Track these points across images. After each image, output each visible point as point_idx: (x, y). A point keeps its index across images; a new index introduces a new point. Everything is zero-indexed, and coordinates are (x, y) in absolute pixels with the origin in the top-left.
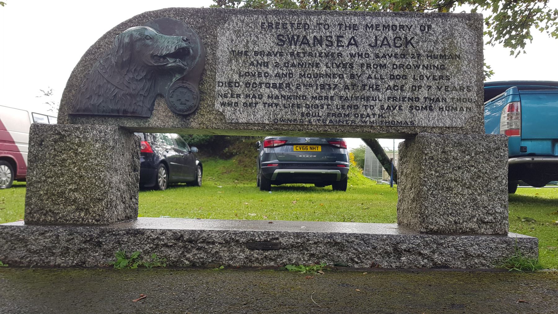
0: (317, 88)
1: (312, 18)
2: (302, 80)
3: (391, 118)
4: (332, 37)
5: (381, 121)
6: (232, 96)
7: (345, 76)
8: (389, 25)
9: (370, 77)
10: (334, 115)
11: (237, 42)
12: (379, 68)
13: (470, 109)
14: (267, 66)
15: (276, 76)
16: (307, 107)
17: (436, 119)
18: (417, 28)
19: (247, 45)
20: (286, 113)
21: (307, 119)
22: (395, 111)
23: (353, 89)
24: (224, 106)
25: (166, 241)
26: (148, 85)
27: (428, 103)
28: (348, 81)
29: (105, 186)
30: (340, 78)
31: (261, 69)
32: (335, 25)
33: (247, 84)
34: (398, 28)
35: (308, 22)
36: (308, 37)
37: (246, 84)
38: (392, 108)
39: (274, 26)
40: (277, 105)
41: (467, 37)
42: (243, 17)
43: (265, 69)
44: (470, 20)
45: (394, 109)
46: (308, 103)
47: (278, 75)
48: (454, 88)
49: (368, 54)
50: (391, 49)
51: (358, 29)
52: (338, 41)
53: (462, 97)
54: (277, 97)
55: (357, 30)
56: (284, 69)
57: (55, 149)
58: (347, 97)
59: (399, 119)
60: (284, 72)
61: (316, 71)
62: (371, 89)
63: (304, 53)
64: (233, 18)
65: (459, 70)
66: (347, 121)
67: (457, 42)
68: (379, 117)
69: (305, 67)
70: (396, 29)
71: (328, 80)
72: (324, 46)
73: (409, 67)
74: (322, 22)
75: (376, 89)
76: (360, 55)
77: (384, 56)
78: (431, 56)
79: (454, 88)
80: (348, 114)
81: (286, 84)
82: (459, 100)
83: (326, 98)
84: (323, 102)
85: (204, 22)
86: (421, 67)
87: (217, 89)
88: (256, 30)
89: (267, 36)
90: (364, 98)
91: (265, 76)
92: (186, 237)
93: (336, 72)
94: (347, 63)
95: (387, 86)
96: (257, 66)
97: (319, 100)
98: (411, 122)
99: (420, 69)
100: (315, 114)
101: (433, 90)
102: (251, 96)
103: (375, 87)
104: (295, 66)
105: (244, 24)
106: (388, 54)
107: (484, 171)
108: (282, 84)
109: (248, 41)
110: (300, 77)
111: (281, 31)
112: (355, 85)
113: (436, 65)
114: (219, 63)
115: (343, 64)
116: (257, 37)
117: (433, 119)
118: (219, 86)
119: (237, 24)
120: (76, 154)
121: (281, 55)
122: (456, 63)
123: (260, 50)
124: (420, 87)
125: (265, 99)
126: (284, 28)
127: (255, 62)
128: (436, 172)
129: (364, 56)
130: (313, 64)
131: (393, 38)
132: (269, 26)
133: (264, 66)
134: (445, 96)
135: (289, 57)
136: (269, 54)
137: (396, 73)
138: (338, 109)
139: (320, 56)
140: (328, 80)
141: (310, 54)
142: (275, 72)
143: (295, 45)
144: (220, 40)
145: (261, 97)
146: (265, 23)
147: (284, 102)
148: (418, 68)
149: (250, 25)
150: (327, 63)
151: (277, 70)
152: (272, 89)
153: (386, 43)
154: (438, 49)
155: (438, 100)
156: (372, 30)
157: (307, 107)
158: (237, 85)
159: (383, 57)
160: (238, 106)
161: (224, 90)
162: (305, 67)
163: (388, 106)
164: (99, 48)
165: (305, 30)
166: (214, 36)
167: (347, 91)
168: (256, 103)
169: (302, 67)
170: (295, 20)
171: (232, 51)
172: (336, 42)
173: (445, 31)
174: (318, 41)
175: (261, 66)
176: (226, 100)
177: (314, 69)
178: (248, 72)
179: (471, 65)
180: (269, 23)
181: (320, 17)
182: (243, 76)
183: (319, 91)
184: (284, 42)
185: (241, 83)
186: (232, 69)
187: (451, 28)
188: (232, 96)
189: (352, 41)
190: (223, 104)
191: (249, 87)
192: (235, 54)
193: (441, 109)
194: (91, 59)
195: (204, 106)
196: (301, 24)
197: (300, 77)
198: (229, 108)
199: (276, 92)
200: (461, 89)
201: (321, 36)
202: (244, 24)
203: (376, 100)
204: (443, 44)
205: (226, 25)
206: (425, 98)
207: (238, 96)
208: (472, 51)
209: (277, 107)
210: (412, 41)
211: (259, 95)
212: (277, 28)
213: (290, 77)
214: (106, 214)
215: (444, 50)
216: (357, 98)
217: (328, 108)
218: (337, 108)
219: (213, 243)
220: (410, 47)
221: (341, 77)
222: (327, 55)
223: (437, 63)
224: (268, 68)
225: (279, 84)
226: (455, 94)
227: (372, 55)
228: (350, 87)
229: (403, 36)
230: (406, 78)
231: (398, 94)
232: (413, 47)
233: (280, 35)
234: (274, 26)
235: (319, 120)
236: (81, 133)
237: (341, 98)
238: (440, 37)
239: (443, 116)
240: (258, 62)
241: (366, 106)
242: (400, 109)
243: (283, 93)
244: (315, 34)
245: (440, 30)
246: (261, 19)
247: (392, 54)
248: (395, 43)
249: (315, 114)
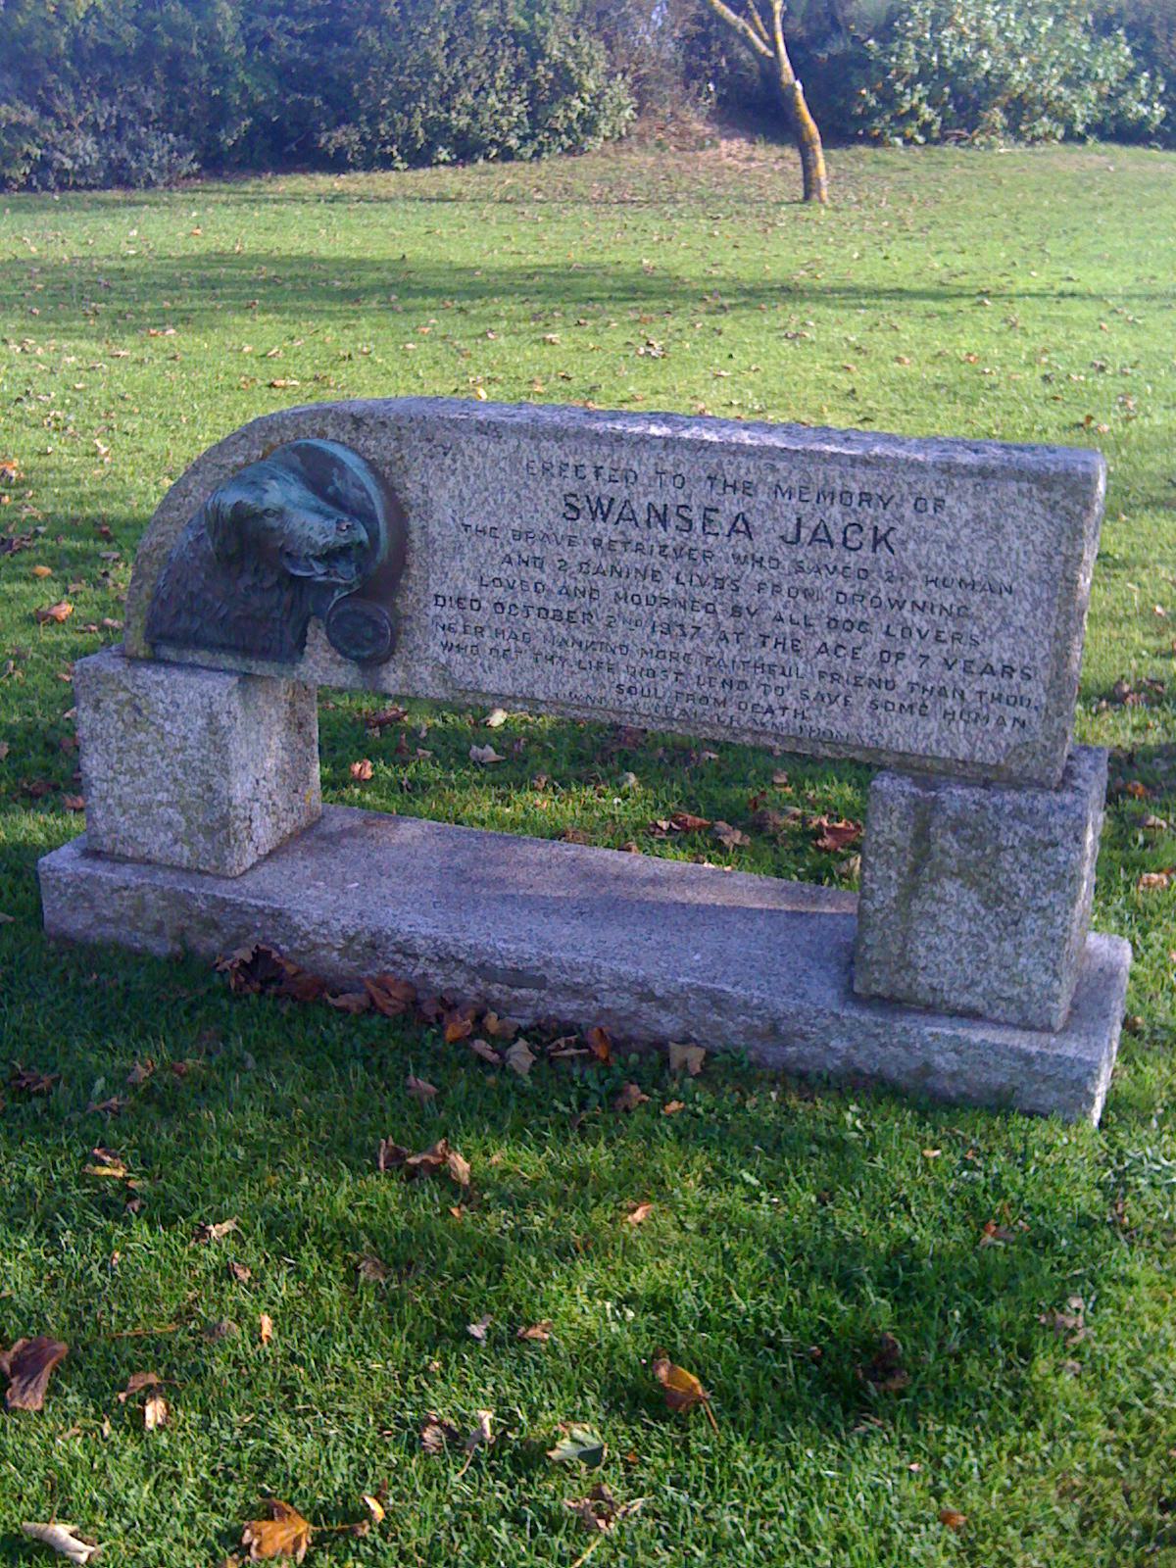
7: (719, 608)
10: (691, 697)
13: (1023, 724)
17: (934, 737)
20: (584, 681)
22: (834, 706)
26: (287, 598)
27: (916, 697)
28: (728, 624)
35: (635, 468)
41: (1037, 537)
48: (989, 670)
50: (834, 554)
53: (1006, 692)
56: (580, 576)
59: (842, 728)
63: (626, 543)
65: (1006, 624)
72: (671, 530)
74: (668, 467)
79: (989, 670)
80: (724, 702)
83: (674, 656)
84: (666, 664)
86: (908, 606)
91: (536, 590)
95: (818, 644)
99: (906, 612)
101: (934, 667)
103: (789, 643)
107: (1014, 890)
111: (571, 484)
117: (927, 736)
119: (472, 459)
123: (525, 528)
124: (900, 656)
127: (514, 556)
131: (841, 525)
132: (545, 470)
134: (961, 685)
137: (842, 614)
141: (639, 548)
142: (560, 584)
147: (580, 656)
153: (822, 535)
155: (942, 692)
167: (723, 644)
170: (601, 454)
179: (1039, 613)
183: (657, 637)
185: (484, 604)
189: (740, 523)
190: (447, 647)
199: (561, 630)
205: (448, 461)
206: (912, 686)
208: (1046, 576)
210: (890, 538)
219: (416, 957)
226: (988, 683)
227: (786, 564)
231: (845, 665)
234: (555, 471)
243: (579, 636)
244: (651, 498)
245: (966, 513)
248: (845, 540)
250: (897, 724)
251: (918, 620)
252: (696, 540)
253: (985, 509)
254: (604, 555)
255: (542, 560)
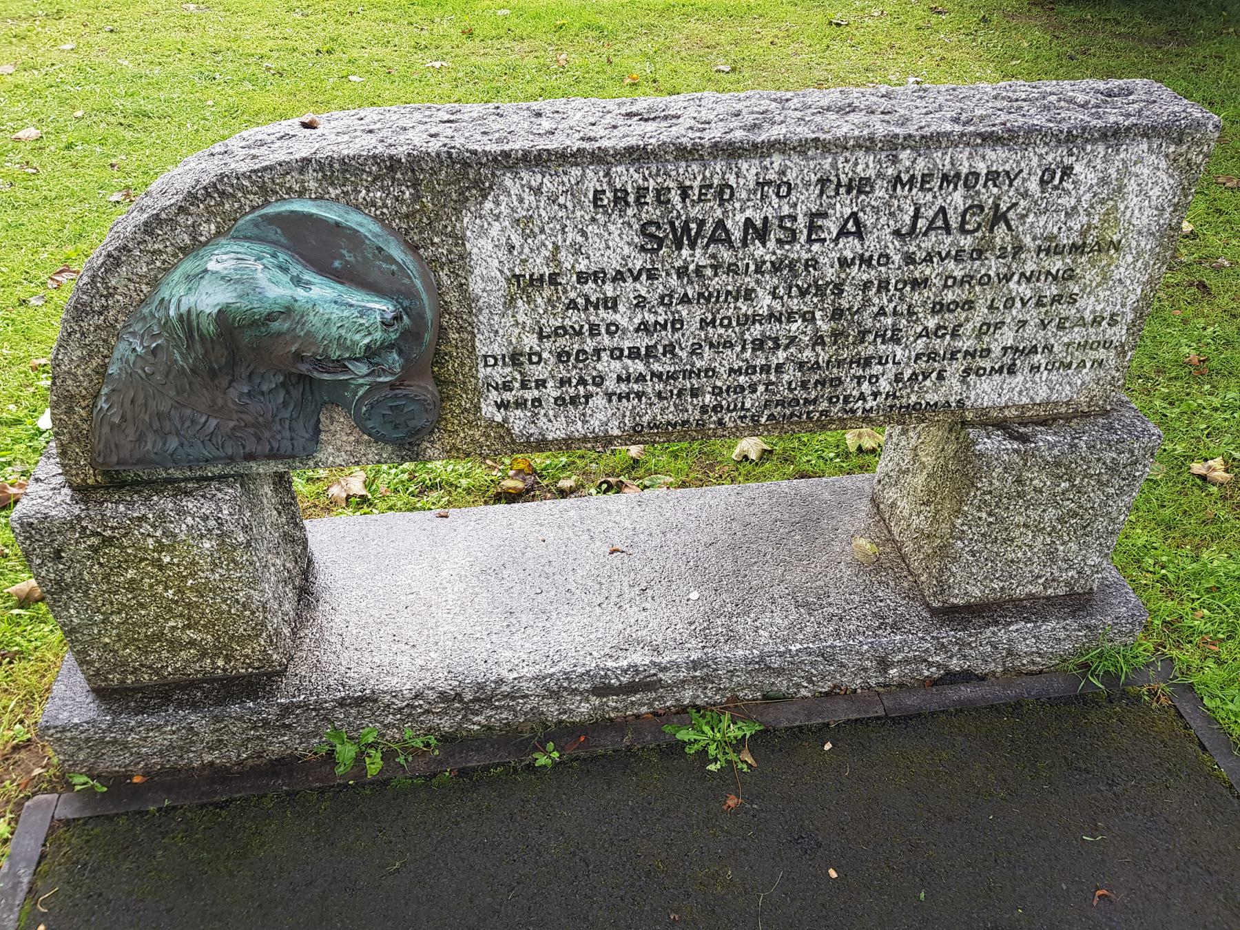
0: (744, 349)
1: (745, 166)
2: (706, 335)
3: (914, 398)
4: (794, 218)
5: (891, 407)
6: (524, 386)
7: (818, 314)
8: (958, 175)
9: (882, 312)
11: (526, 250)
12: (908, 288)
13: (1100, 364)
14: (615, 308)
15: (637, 330)
16: (717, 391)
18: (1033, 178)
19: (554, 258)
21: (714, 418)
22: (928, 383)
23: (835, 343)
24: (506, 409)
25: (426, 707)
27: (1007, 360)
28: (824, 326)
29: (253, 613)
30: (804, 320)
31: (597, 315)
32: (807, 185)
33: (562, 356)
34: (981, 181)
35: (732, 181)
36: (729, 224)
37: (559, 355)
38: (920, 378)
39: (631, 199)
40: (639, 395)
42: (539, 177)
43: (609, 316)
44: (1180, 142)
45: (925, 378)
46: (719, 384)
47: (644, 328)
48: (1081, 322)
49: (887, 257)
50: (950, 239)
51: (872, 190)
52: (812, 228)
54: (641, 378)
55: (867, 193)
56: (661, 310)
57: (101, 565)
58: (817, 363)
60: (661, 320)
61: (744, 308)
62: (879, 340)
63: (715, 268)
64: (508, 182)
66: (809, 413)
67: (1127, 208)
68: (886, 399)
69: (717, 301)
70: (977, 183)
71: (772, 329)
72: (771, 244)
73: (985, 281)
74: (772, 176)
75: (891, 339)
76: (866, 261)
77: (929, 259)
78: (1048, 251)
79: (1081, 322)
81: (665, 347)
82: (1083, 346)
83: (766, 369)
85: (417, 198)
86: (1016, 278)
87: (483, 372)
88: (578, 214)
89: (612, 228)
90: (858, 362)
91: (608, 332)
92: (468, 696)
93: (795, 308)
94: (828, 284)
95: (919, 329)
96: (586, 309)
97: (747, 374)
98: (959, 401)
99: (1012, 285)
100: (736, 405)
101: (1029, 331)
102: (574, 382)
103: (889, 333)
104: (689, 302)
105: (543, 199)
106: (939, 253)
108: (655, 346)
109: (557, 248)
110: (702, 328)
111: (652, 211)
112: (842, 334)
113: (1054, 272)
114: (480, 310)
115: (818, 288)
116: (584, 234)
118: (486, 365)
119: (521, 201)
120: (161, 568)
121: (652, 275)
122: (1104, 262)
123: (593, 268)
124: (999, 325)
125: (610, 384)
126: (660, 202)
127: (581, 301)
128: (990, 515)
129: (874, 262)
130: (738, 292)
131: (961, 209)
132: (616, 200)
133: (606, 308)
134: (1052, 341)
135: (674, 281)
136: (619, 277)
137: (949, 296)
138: (791, 390)
139: (758, 270)
140: (772, 329)
141: (732, 269)
142: (637, 321)
143: (693, 246)
144: (475, 250)
145: (599, 380)
146: (604, 192)
147: (659, 387)
148: (1008, 281)
149: (561, 200)
150: (776, 288)
151: (640, 316)
152: (629, 362)
153: (939, 223)
154: (1070, 229)
155: (1034, 350)
156: (910, 190)
157: (717, 391)
158: (535, 359)
159: (924, 260)
160: (540, 405)
161: (500, 373)
162: (717, 301)
163: (914, 373)
164: (112, 295)
165: (722, 202)
166: (456, 237)
167: (818, 349)
168: (588, 397)
169: (708, 300)
170: (693, 175)
171: (514, 276)
172: (805, 231)
173: (1103, 181)
174: (759, 232)
175: (596, 307)
176: (508, 396)
177: (739, 304)
178: (563, 327)
179: (1139, 264)
180: (616, 191)
181: (767, 162)
182: (549, 337)
183: (748, 355)
184: (660, 242)
185: (545, 355)
186: (517, 323)
187: (1125, 171)
188: (524, 386)
191: (568, 360)
192: (525, 284)
193: (1035, 369)
194: (97, 327)
195: (452, 411)
196: (710, 186)
197: (702, 328)
198: (518, 412)
199: (638, 367)
200: (1094, 320)
201: (766, 218)
202: (543, 199)
203: (887, 362)
204: (1089, 215)
205: (489, 205)
206: (1005, 349)
207: (541, 384)
209: (640, 400)
210: (1011, 215)
211: (594, 378)
212: (639, 203)
213: (674, 330)
214: (275, 656)
215: (1084, 233)
216: (840, 364)
217: (766, 390)
218: (789, 388)
219: (526, 696)
220: (1001, 230)
221: (808, 318)
222: (776, 268)
223: (1059, 264)
224: (616, 312)
225: (647, 348)
226: (1077, 335)
227: (897, 258)
228: (827, 340)
229: (990, 201)
230: (970, 308)
231: (940, 345)
232: (1009, 228)
233: (650, 223)
234: (631, 199)
235: (742, 418)
236: (154, 526)
237: (801, 365)
238: (1088, 196)
239: (1034, 382)
240: (587, 300)
241: (859, 378)
242: (940, 377)
243: (656, 367)
244: (749, 213)
245: (1092, 178)
246: (593, 179)
247: (948, 253)
248: (963, 222)
249: (736, 405)
250: (985, 386)
251: (1025, 290)
252: (798, 251)
253: (1112, 171)
254: (690, 282)
255: (615, 301)
